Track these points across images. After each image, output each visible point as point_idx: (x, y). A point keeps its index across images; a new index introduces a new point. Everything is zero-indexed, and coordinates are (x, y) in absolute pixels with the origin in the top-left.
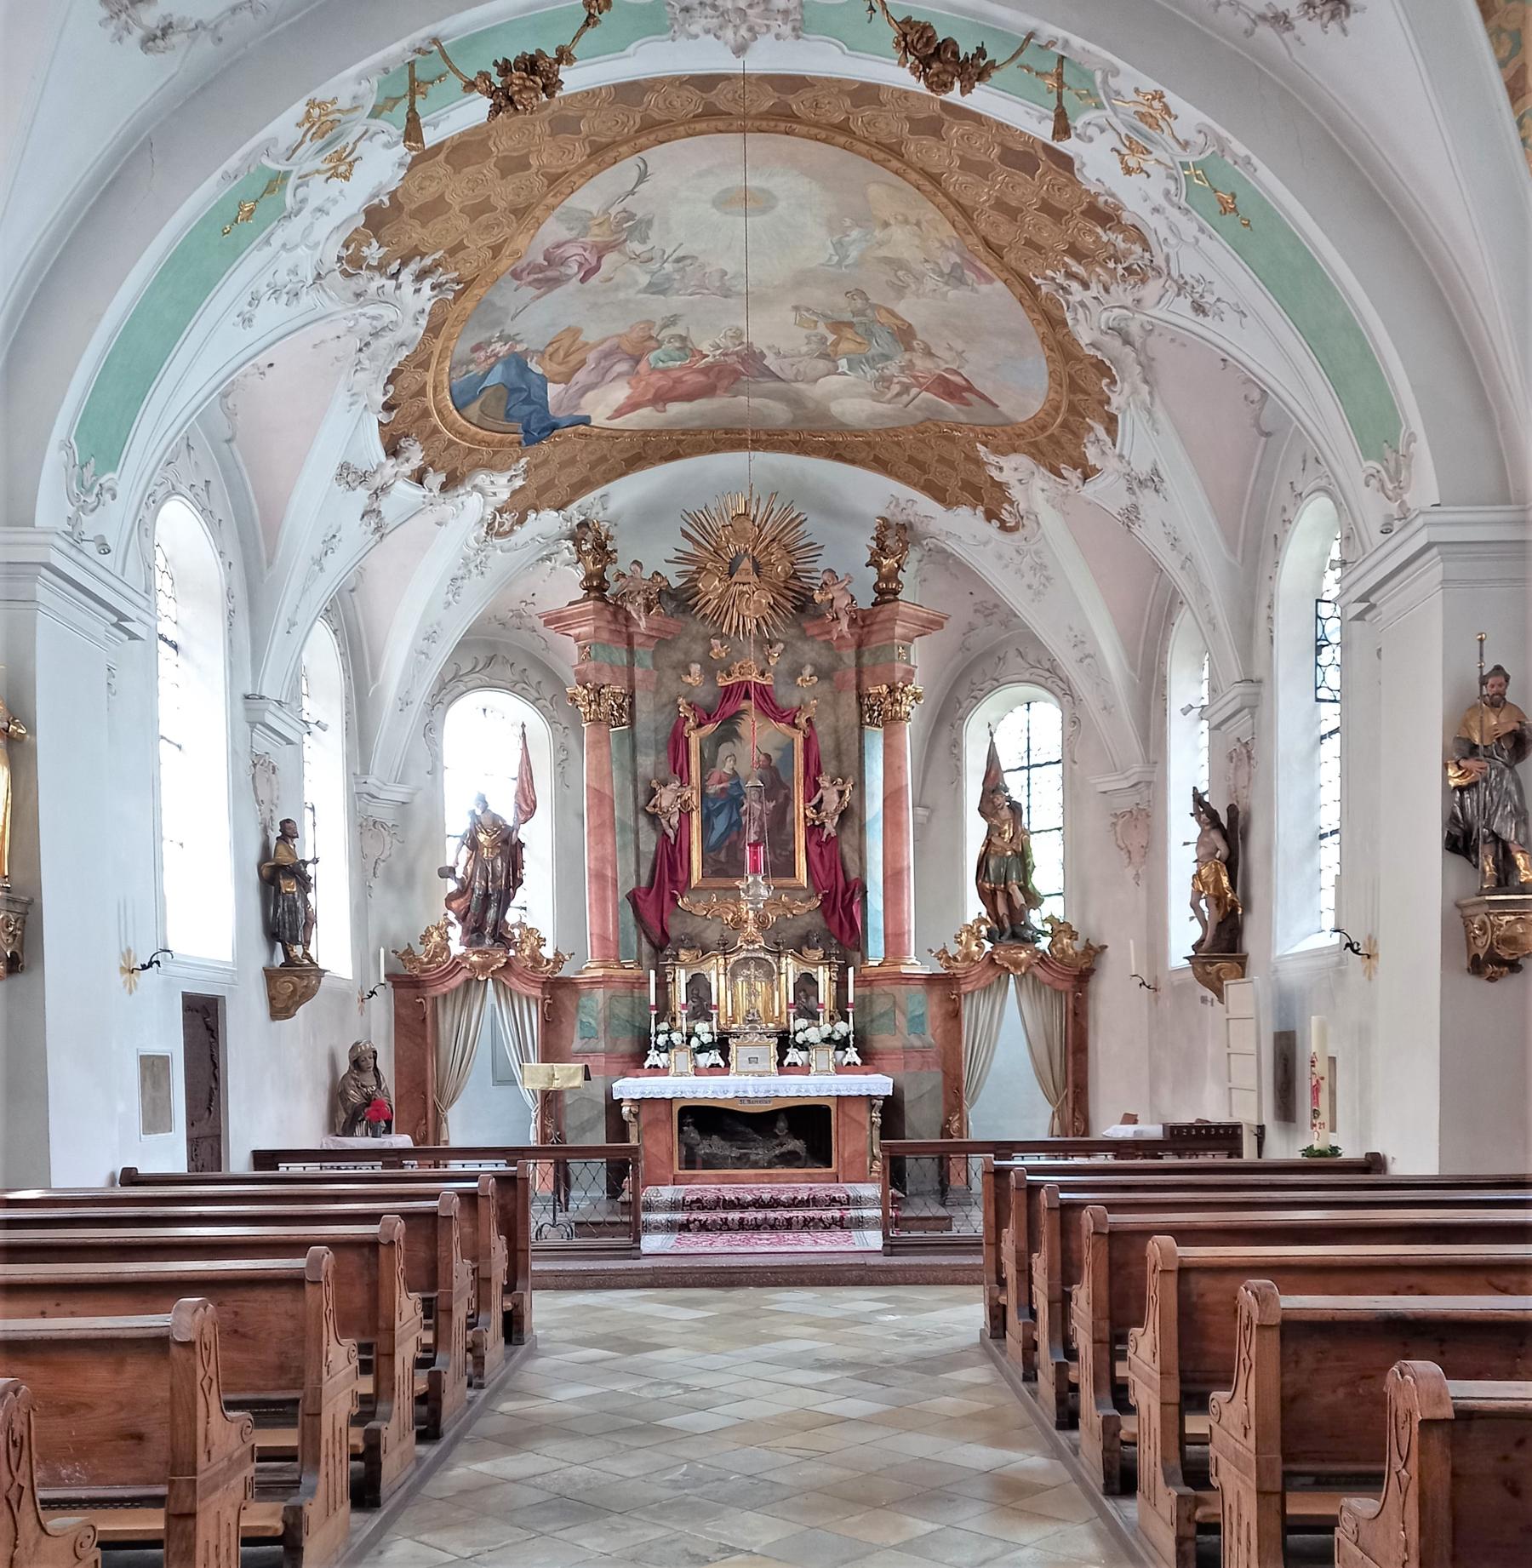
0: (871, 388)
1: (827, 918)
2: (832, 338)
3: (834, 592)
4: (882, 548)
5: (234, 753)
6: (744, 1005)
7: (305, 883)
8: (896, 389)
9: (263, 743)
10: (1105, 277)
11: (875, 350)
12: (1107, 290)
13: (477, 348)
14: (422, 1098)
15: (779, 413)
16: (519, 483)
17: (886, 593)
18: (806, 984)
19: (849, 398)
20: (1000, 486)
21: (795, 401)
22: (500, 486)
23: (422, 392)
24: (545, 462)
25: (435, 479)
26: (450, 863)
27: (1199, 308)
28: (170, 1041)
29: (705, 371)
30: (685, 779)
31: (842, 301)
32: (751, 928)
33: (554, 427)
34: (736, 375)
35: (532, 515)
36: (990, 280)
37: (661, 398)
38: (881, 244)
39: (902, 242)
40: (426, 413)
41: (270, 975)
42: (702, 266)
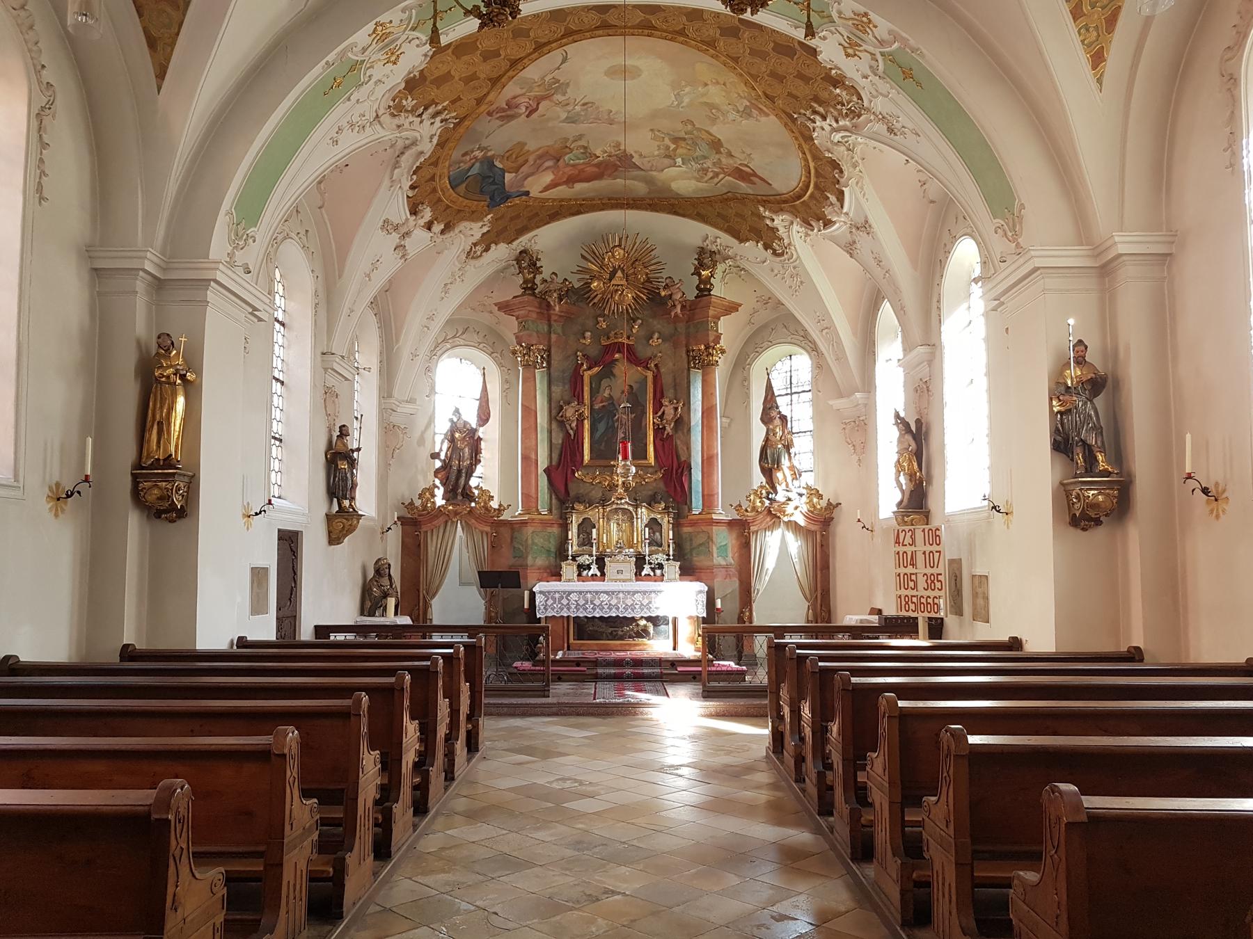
0: (696, 174)
1: (666, 484)
2: (673, 146)
3: (674, 290)
4: (701, 265)
5: (314, 386)
6: (615, 538)
7: (353, 463)
8: (710, 175)
9: (332, 381)
10: (836, 113)
11: (698, 153)
12: (837, 121)
13: (465, 154)
14: (416, 596)
15: (640, 188)
16: (485, 229)
17: (704, 290)
18: (654, 525)
19: (682, 179)
20: (774, 230)
21: (650, 182)
22: (475, 230)
23: (432, 178)
24: (502, 217)
25: (438, 227)
26: (437, 450)
27: (890, 130)
28: (269, 559)
29: (598, 165)
30: (581, 401)
31: (680, 126)
32: (620, 490)
33: (507, 197)
34: (616, 168)
35: (493, 246)
36: (767, 115)
37: (571, 181)
38: (703, 95)
39: (715, 94)
40: (434, 190)
41: (329, 518)
42: (597, 108)
